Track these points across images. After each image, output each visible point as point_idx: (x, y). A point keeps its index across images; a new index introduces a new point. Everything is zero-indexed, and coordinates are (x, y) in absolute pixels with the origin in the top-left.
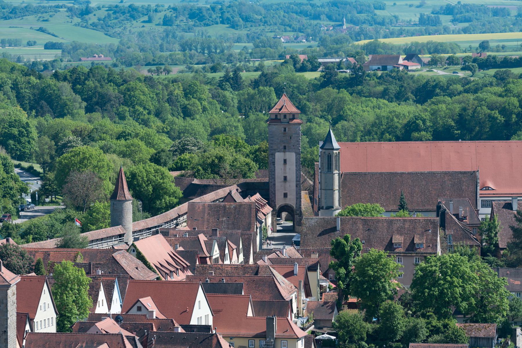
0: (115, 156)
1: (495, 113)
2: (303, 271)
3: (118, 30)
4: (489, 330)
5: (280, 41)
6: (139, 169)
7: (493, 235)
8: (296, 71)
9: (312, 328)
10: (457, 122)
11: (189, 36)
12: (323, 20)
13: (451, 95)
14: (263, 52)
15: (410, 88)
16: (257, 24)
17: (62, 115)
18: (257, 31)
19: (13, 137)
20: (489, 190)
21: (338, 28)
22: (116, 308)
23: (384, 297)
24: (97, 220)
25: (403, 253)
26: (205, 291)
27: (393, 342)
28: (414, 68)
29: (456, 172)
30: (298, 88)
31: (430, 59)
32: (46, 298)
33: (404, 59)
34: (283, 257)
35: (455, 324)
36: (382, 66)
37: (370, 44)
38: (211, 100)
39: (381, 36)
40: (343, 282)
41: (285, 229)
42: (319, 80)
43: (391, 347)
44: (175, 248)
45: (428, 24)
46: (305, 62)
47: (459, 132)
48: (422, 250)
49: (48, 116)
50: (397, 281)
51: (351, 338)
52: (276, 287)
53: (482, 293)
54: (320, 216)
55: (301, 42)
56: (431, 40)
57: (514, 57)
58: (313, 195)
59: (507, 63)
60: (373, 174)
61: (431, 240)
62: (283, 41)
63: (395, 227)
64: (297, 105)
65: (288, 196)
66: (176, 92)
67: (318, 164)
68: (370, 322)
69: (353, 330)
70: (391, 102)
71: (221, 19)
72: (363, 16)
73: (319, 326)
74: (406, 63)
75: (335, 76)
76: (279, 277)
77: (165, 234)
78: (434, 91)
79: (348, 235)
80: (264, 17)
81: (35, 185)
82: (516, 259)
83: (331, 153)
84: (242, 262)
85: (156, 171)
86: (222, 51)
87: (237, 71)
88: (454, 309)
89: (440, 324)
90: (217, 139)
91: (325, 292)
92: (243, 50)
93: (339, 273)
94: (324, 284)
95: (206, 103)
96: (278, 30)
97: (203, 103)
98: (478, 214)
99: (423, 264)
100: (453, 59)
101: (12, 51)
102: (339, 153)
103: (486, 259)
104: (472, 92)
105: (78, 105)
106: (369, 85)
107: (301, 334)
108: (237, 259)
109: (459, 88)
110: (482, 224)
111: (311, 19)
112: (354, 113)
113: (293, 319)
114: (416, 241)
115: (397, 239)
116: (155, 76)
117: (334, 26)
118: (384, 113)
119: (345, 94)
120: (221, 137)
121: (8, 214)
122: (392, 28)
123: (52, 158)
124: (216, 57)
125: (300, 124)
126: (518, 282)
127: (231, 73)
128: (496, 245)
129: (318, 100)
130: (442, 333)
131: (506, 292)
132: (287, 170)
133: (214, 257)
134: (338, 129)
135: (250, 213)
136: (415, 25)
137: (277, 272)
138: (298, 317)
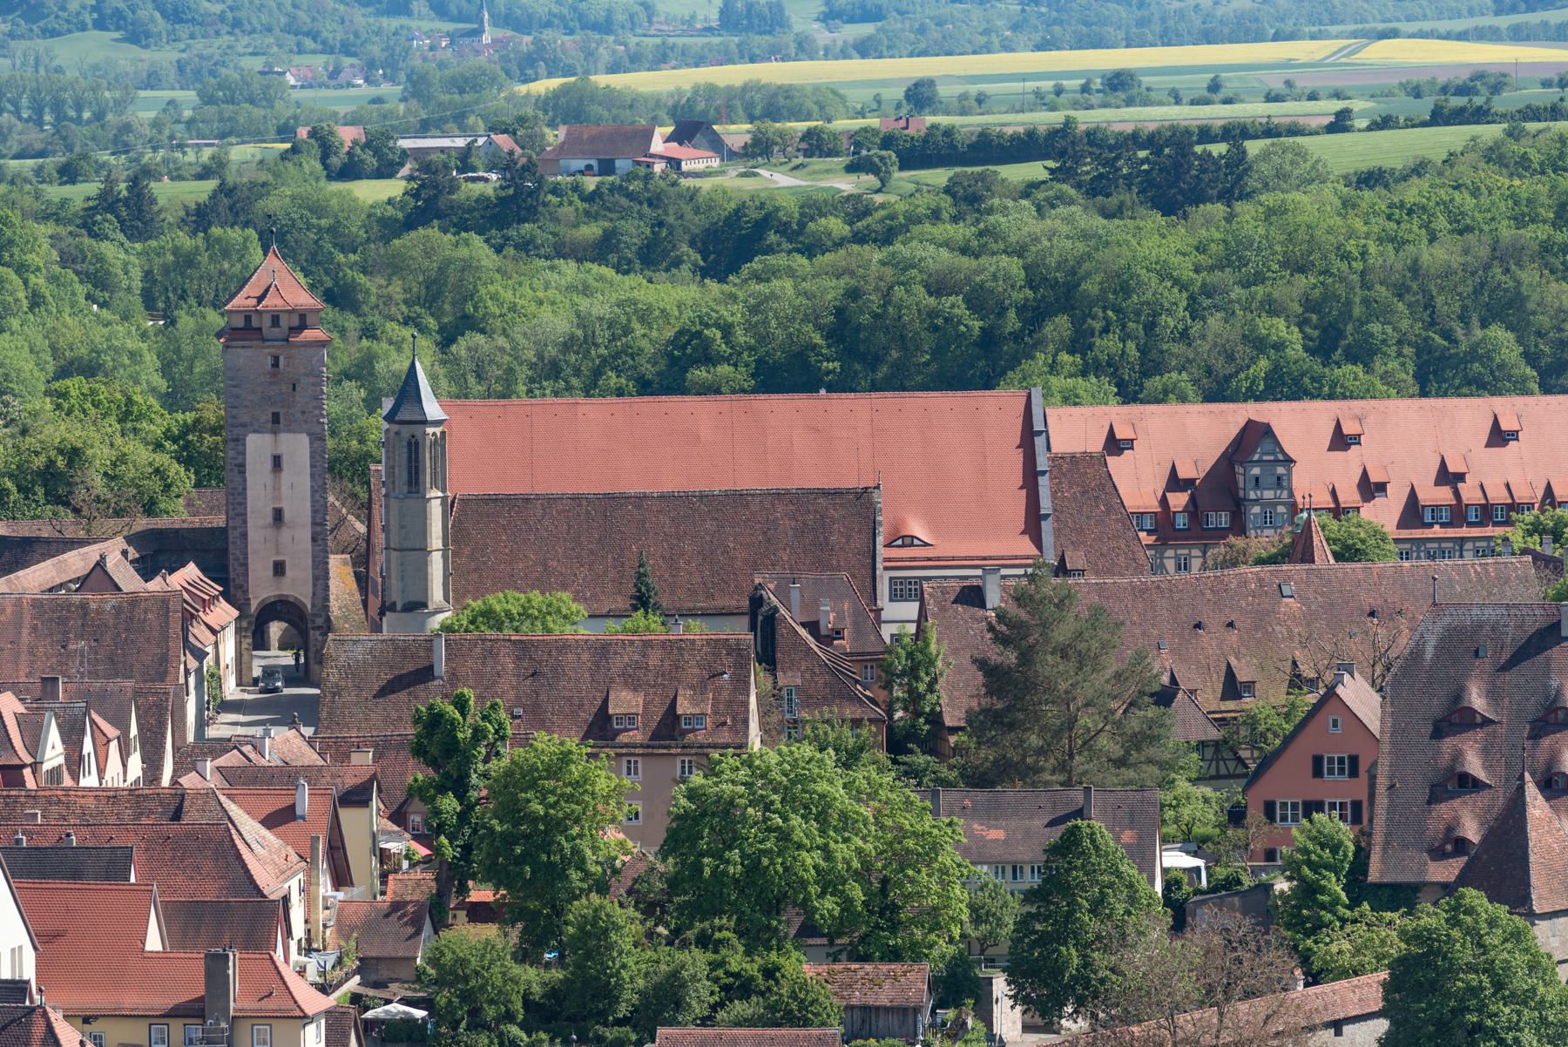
1: (953, 306)
2: (326, 806)
4: (908, 984)
5: (283, 86)
7: (922, 687)
8: (329, 178)
9: (353, 984)
10: (832, 335)
12: (421, 18)
13: (809, 251)
14: (230, 119)
15: (686, 230)
16: (211, 31)
18: (210, 50)
20: (912, 545)
21: (467, 40)
23: (579, 884)
25: (642, 746)
27: (606, 1025)
28: (699, 166)
29: (810, 492)
30: (333, 230)
31: (748, 138)
33: (668, 140)
34: (263, 762)
35: (803, 968)
36: (600, 161)
37: (564, 91)
38: (57, 269)
39: (601, 66)
40: (451, 838)
42: (402, 206)
43: (600, 1039)
46: (358, 150)
47: (837, 364)
48: (701, 737)
50: (619, 835)
51: (475, 1013)
52: (239, 856)
53: (884, 867)
54: (386, 634)
55: (350, 85)
56: (754, 77)
57: (1009, 131)
58: (367, 568)
59: (991, 149)
60: (550, 500)
61: (730, 703)
62: (292, 81)
63: (617, 663)
64: (329, 283)
65: (288, 573)
67: (378, 469)
68: (536, 961)
69: (482, 988)
70: (626, 273)
71: (95, 16)
73: (374, 977)
74: (674, 149)
75: (449, 193)
76: (248, 826)
78: (761, 238)
79: (466, 691)
80: (231, 9)
82: (996, 761)
83: (419, 435)
84: (137, 781)
86: (99, 116)
88: (797, 922)
89: (752, 968)
90: (64, 395)
91: (396, 872)
92: (164, 111)
93: (437, 812)
94: (394, 846)
95: (41, 281)
96: (276, 49)
97: (33, 279)
98: (879, 621)
99: (697, 779)
100: (819, 139)
102: (443, 433)
103: (904, 764)
104: (875, 241)
106: (557, 220)
109: (836, 226)
110: (889, 651)
111: (378, 13)
112: (510, 309)
113: (294, 956)
114: (684, 707)
115: (624, 702)
117: (452, 37)
118: (599, 307)
119: (477, 248)
120: (74, 385)
122: (637, 39)
124: (79, 133)
125: (322, 344)
126: (998, 834)
127: (123, 186)
128: (935, 719)
129: (395, 267)
130: (762, 994)
131: (959, 866)
132: (285, 490)
133: (46, 767)
134: (456, 361)
135: (165, 627)
136: (709, 30)
137: (241, 812)
138: (308, 949)
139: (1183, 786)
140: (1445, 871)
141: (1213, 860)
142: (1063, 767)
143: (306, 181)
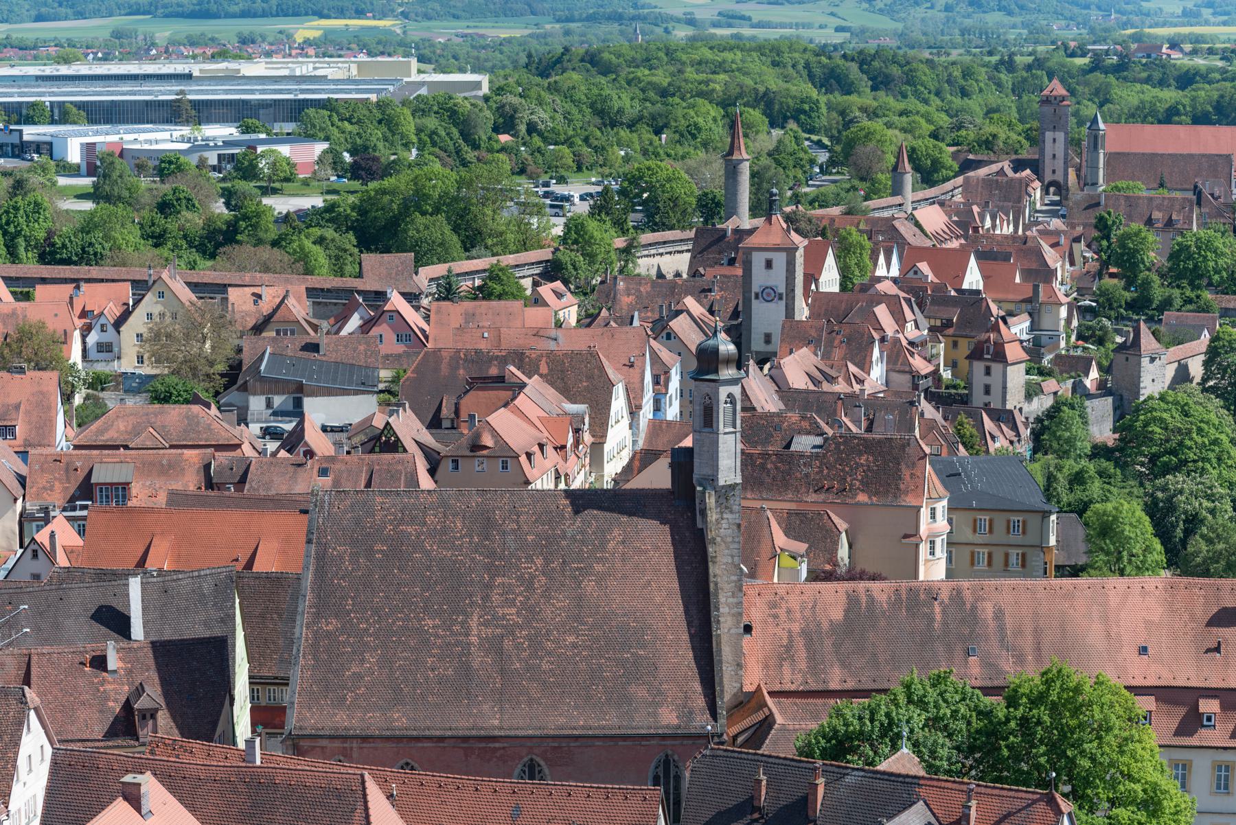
0: (897, 132)
3: (903, 15)
6: (918, 143)
10: (1214, 108)
11: (968, 22)
13: (1209, 83)
17: (849, 93)
19: (805, 112)
22: (895, 272)
24: (879, 190)
26: (978, 258)
30: (1068, 72)
32: (830, 260)
35: (1207, 295)
37: (1135, 33)
41: (1053, 203)
44: (950, 218)
45: (1190, 16)
49: (837, 94)
50: (1154, 253)
51: (1110, 305)
60: (1135, 154)
63: (1155, 203)
66: (955, 73)
67: (1085, 143)
72: (1129, 8)
74: (1169, 51)
76: (1046, 248)
77: (942, 204)
81: (823, 157)
85: (934, 146)
87: (1011, 55)
89: (1193, 295)
94: (1087, 255)
99: (1180, 239)
101: (805, 33)
105: (865, 83)
107: (1064, 300)
108: (1008, 230)
115: (1157, 215)
116: (936, 59)
118: (1147, 97)
119: (1111, 79)
120: (996, 116)
121: (798, 183)
123: (839, 132)
124: (993, 42)
129: (1087, 84)
143: (1060, 57)
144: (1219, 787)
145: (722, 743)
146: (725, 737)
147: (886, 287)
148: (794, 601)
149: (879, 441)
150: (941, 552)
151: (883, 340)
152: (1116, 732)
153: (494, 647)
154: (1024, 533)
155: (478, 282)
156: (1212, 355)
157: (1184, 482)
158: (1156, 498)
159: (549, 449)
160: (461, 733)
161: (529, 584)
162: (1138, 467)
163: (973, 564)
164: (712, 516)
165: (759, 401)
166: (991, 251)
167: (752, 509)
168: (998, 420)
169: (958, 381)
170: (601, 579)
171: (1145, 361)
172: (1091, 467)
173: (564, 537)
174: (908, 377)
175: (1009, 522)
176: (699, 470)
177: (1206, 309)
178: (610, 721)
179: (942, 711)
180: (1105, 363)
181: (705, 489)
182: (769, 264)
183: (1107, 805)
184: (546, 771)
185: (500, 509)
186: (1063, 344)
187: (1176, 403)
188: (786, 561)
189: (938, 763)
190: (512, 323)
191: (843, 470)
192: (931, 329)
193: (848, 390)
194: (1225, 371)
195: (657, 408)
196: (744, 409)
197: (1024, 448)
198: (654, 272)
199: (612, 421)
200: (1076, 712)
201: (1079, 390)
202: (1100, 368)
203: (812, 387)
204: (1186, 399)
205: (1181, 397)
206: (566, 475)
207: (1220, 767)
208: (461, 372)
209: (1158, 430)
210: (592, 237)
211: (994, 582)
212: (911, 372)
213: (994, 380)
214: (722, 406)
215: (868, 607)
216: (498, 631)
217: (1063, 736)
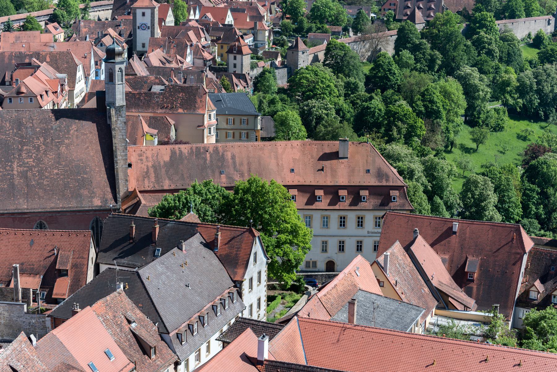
2: (269, 4)
4: (340, 29)
22: (197, 17)
32: (170, 12)
35: (327, 26)
76: (260, 7)
89: (320, 26)
94: (277, 10)
99: (315, 3)
138: (267, 22)
139: (374, 6)
140: (405, 18)
141: (377, 15)
142: (359, 3)
144: (324, 226)
145: (120, 212)
146: (121, 210)
147: (193, 24)
148: (149, 154)
149: (187, 87)
150: (213, 133)
151: (191, 45)
152: (279, 203)
153: (23, 175)
154: (247, 124)
155: (22, 24)
156: (328, 50)
157: (315, 103)
158: (304, 109)
159: (50, 93)
160: (11, 212)
161: (38, 149)
162: (297, 97)
163: (226, 137)
164: (114, 119)
165: (138, 71)
166: (237, 8)
167: (134, 116)
168: (239, 78)
169: (223, 62)
170: (68, 146)
171: (300, 54)
172: (277, 97)
173: (52, 129)
174: (202, 61)
175: (241, 120)
176: (108, 99)
177: (326, 32)
178: (73, 205)
179: (208, 197)
180: (284, 54)
181: (110, 108)
182: (144, 14)
183: (276, 233)
184: (47, 226)
185: (25, 118)
186: (267, 47)
187: (312, 70)
188: (149, 137)
189: (207, 218)
190: (35, 41)
191: (172, 99)
192: (212, 41)
193: (177, 66)
194: (333, 58)
195: (97, 75)
196: (126, 75)
197: (250, 90)
198: (96, 18)
199: (77, 81)
200: (263, 196)
201: (273, 66)
202: (282, 56)
203: (162, 65)
204: (316, 69)
205: (315, 68)
206: (58, 104)
207: (324, 217)
208: (13, 61)
209: (305, 82)
210: (70, 4)
211: (231, 144)
212: (203, 59)
213: (238, 62)
214: (117, 73)
215: (179, 155)
216: (25, 169)
217: (257, 205)
